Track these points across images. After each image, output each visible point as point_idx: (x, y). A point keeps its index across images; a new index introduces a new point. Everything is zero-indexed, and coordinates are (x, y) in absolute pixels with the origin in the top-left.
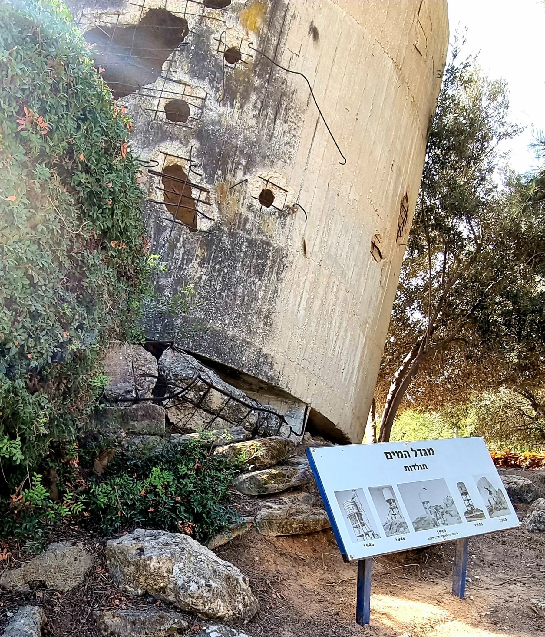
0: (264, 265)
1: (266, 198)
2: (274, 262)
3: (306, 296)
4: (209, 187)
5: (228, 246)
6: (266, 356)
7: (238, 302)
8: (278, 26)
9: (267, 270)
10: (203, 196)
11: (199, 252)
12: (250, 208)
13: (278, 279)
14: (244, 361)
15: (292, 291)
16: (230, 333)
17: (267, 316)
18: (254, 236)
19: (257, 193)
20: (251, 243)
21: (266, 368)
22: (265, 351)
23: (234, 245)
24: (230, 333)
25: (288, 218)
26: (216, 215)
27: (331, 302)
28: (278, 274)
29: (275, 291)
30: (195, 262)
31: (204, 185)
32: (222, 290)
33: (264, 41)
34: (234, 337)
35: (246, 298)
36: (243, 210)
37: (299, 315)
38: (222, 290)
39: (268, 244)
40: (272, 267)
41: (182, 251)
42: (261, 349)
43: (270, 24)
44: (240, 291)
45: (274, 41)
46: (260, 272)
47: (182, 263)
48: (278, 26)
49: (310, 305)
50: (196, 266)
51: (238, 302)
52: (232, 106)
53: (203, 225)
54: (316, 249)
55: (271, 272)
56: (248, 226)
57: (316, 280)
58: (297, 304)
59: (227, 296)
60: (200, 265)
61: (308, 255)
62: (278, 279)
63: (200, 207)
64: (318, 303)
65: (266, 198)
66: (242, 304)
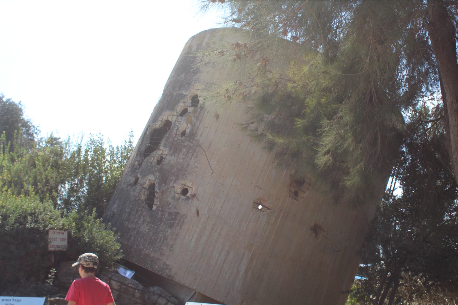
0: (174, 223)
1: (185, 192)
2: (179, 221)
4: (158, 191)
5: (159, 216)
6: (168, 265)
7: (159, 240)
8: (200, 118)
9: (175, 225)
11: (148, 219)
12: (174, 197)
13: (181, 228)
14: (156, 268)
16: (152, 255)
17: (171, 247)
19: (179, 191)
20: (170, 214)
21: (167, 271)
23: (162, 215)
24: (152, 255)
25: (190, 200)
26: (158, 203)
28: (181, 226)
29: (178, 235)
30: (146, 224)
32: (152, 236)
33: (193, 125)
34: (153, 257)
35: (162, 239)
36: (170, 200)
38: (152, 236)
39: (178, 213)
40: (178, 224)
41: (142, 220)
42: (166, 262)
43: (197, 118)
44: (160, 235)
45: (197, 125)
46: (171, 226)
51: (159, 240)
52: (175, 156)
53: (154, 208)
55: (177, 226)
56: (170, 206)
60: (147, 225)
61: (200, 215)
62: (181, 228)
63: (155, 200)
65: (185, 192)
66: (160, 241)
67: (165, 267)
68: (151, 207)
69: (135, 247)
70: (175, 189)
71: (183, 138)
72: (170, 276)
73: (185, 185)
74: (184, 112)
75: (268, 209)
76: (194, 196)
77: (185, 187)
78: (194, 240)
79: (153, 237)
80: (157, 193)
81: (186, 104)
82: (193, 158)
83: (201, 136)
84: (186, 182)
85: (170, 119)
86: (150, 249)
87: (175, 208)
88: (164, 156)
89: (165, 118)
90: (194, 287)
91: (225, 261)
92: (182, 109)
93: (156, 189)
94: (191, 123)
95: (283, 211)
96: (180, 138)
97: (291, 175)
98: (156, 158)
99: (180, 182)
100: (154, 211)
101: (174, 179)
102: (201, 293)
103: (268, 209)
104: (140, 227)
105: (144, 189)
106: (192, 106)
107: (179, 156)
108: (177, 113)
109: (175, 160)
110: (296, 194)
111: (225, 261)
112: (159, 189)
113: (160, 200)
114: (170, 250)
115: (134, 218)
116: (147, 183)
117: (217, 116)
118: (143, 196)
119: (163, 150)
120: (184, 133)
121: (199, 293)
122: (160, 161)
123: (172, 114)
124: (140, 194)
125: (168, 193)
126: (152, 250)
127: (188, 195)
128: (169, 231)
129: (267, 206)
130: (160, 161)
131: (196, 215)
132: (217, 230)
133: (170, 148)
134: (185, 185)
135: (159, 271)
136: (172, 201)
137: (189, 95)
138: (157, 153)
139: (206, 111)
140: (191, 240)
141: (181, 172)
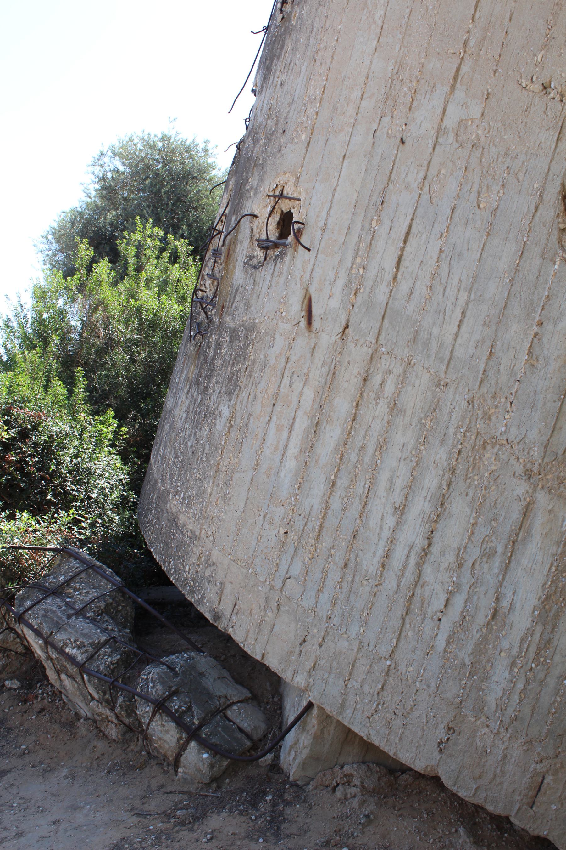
2: (254, 362)
3: (302, 424)
15: (274, 418)
20: (234, 335)
22: (216, 555)
27: (377, 427)
34: (184, 525)
35: (207, 447)
37: (282, 474)
39: (252, 328)
49: (309, 448)
54: (334, 303)
58: (281, 447)
61: (316, 324)
64: (332, 435)
67: (208, 573)
70: (256, 221)
72: (217, 617)
73: (281, 196)
77: (285, 206)
78: (293, 450)
84: (281, 179)
91: (426, 551)
102: (328, 709)
111: (426, 551)
114: (224, 498)
121: (321, 709)
126: (183, 498)
131: (303, 324)
134: (281, 196)
135: (192, 592)
140: (286, 446)
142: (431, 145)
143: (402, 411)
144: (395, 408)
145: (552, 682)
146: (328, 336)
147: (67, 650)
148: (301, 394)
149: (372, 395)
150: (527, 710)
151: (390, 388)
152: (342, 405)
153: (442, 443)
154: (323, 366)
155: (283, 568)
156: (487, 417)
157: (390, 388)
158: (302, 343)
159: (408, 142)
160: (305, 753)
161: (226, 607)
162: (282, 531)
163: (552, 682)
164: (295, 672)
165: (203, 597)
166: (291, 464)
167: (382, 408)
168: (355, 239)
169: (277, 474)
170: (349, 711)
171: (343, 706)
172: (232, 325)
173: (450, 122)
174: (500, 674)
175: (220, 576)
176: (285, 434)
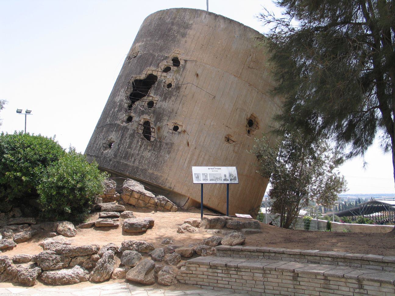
1: (176, 128)
3: (188, 160)
10: (153, 131)
14: (160, 183)
18: (168, 141)
19: (172, 127)
20: (167, 144)
22: (168, 178)
23: (160, 145)
26: (156, 136)
31: (154, 127)
35: (163, 162)
36: (165, 134)
37: (184, 166)
46: (169, 153)
47: (143, 152)
48: (184, 76)
50: (147, 152)
53: (152, 139)
54: (193, 143)
57: (193, 154)
59: (156, 161)
65: (176, 128)
68: (148, 138)
69: (141, 167)
70: (169, 126)
71: (170, 89)
73: (176, 124)
74: (167, 70)
75: (234, 142)
76: (185, 131)
79: (155, 161)
80: (153, 128)
81: (169, 64)
82: (181, 105)
83: (186, 89)
85: (155, 73)
86: (154, 169)
87: (170, 140)
88: (155, 102)
89: (149, 72)
90: (189, 195)
92: (165, 67)
93: (152, 126)
94: (177, 79)
95: (242, 144)
96: (167, 89)
97: (247, 119)
98: (146, 103)
99: (172, 121)
100: (152, 142)
101: (167, 119)
103: (234, 142)
104: (142, 153)
105: (140, 126)
106: (174, 65)
107: (169, 102)
108: (161, 69)
109: (166, 105)
110: (249, 132)
112: (155, 126)
113: (157, 134)
115: (136, 147)
116: (142, 121)
117: (197, 75)
118: (140, 130)
119: (153, 95)
120: (170, 85)
121: (191, 198)
122: (151, 104)
123: (158, 70)
124: (138, 128)
125: (164, 129)
127: (179, 130)
128: (168, 156)
129: (233, 140)
130: (151, 104)
131: (187, 145)
132: (202, 155)
133: (161, 96)
134: (176, 124)
135: (162, 185)
136: (167, 135)
137: (171, 57)
138: (147, 99)
139: (188, 71)
140: (185, 162)
141: (172, 113)
142: (209, 126)
143: (205, 159)
144: (204, 159)
145: (221, 192)
146: (192, 148)
147: (146, 195)
148: (187, 155)
149: (200, 157)
150: (218, 195)
151: (203, 156)
152: (195, 158)
153: (210, 163)
154: (192, 151)
155: (185, 180)
156: (216, 161)
157: (203, 156)
158: (187, 148)
159: (205, 125)
160: (187, 206)
161: (172, 186)
162: (185, 174)
163: (221, 192)
164: (188, 194)
165: (166, 185)
166: (186, 165)
167: (202, 159)
168: (197, 135)
169: (183, 166)
170: (196, 198)
171: (196, 197)
172: (166, 142)
173: (212, 124)
174: (216, 191)
175: (170, 182)
176: (184, 161)
